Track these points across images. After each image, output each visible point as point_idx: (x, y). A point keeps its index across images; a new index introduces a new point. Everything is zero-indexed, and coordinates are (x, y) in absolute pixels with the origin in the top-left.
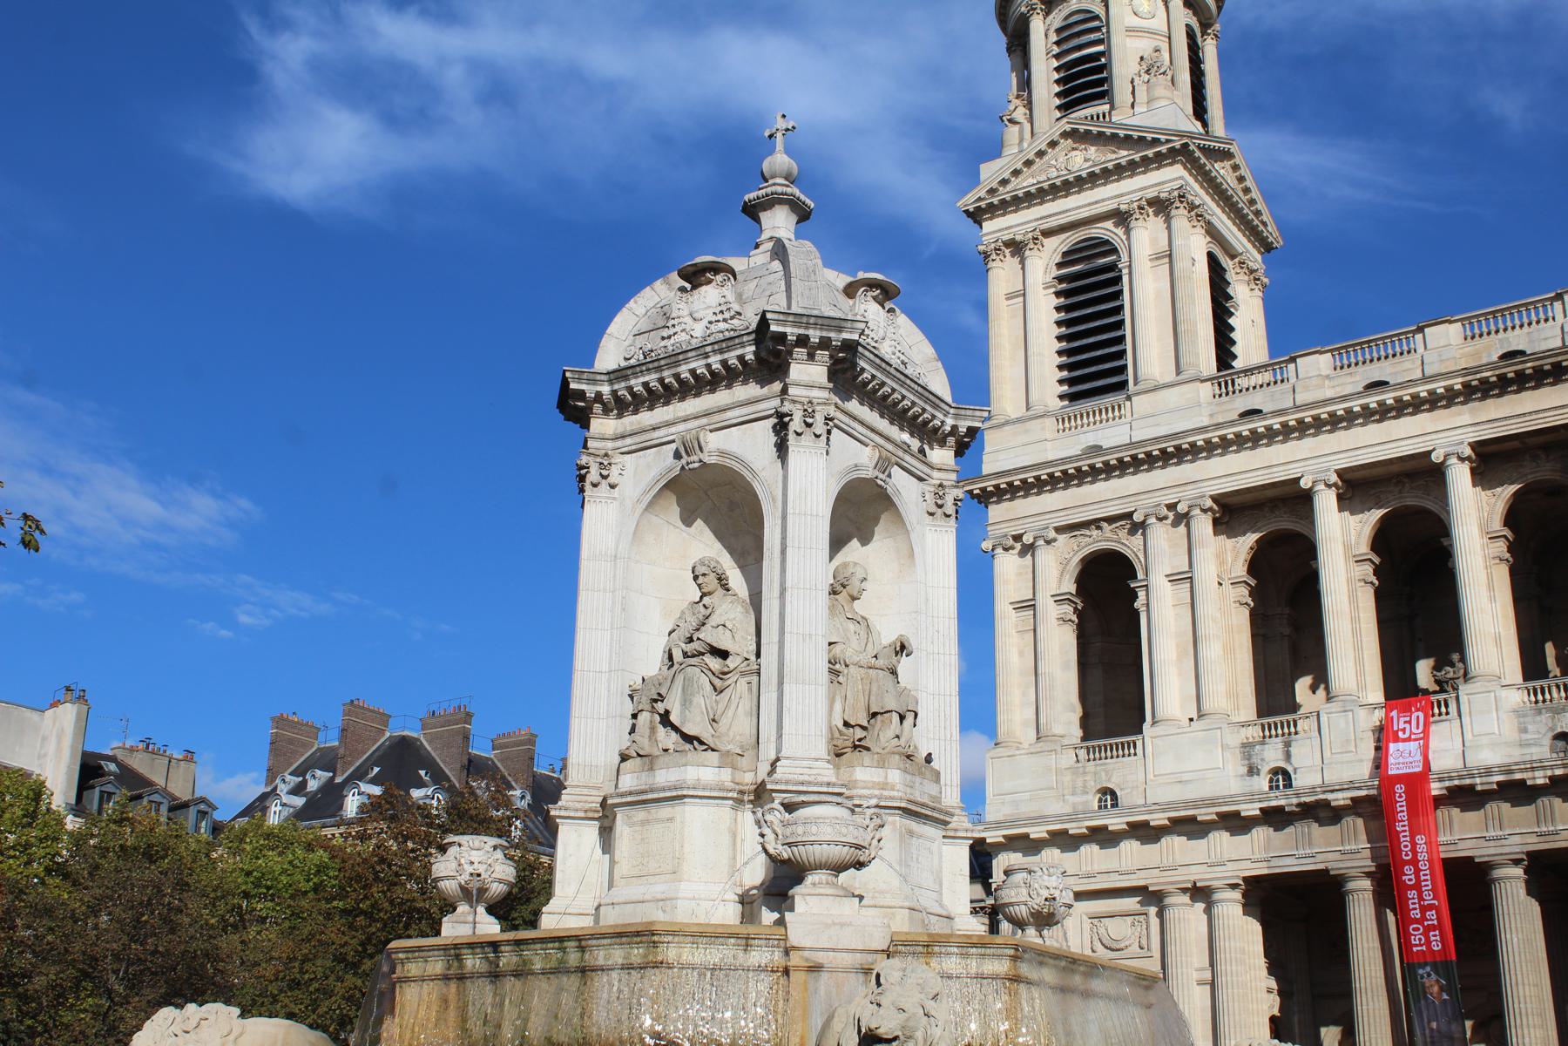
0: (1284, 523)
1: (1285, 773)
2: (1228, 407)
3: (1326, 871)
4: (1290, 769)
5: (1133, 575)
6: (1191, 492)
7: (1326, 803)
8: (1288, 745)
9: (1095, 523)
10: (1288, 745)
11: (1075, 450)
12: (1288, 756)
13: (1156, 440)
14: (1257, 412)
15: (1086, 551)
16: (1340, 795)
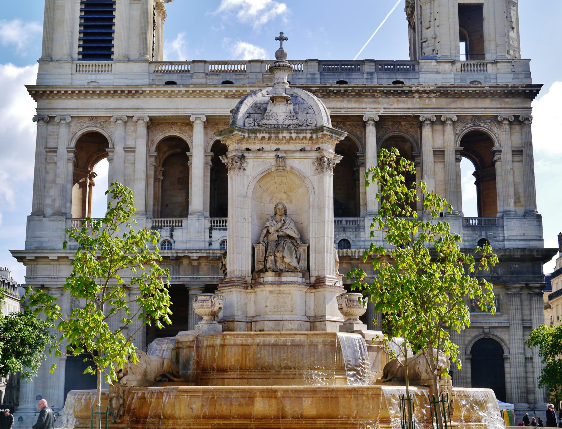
0: (175, 132)
1: (169, 242)
2: (161, 77)
3: (183, 285)
4: (172, 241)
5: (108, 146)
6: (139, 113)
7: (189, 257)
8: (172, 230)
9: (91, 118)
10: (172, 230)
11: (85, 82)
12: (172, 236)
13: (128, 86)
14: (174, 83)
15: (85, 130)
16: (195, 255)
